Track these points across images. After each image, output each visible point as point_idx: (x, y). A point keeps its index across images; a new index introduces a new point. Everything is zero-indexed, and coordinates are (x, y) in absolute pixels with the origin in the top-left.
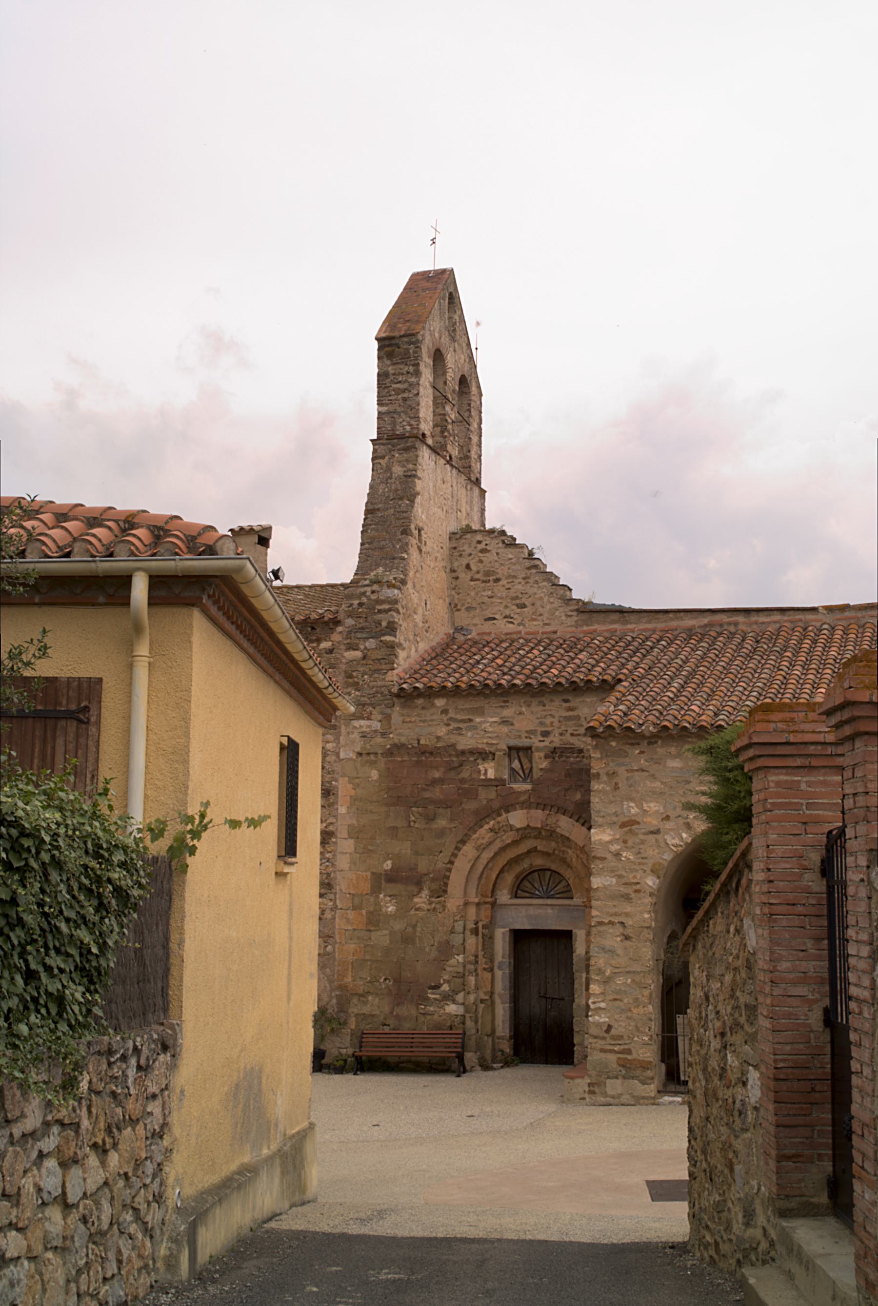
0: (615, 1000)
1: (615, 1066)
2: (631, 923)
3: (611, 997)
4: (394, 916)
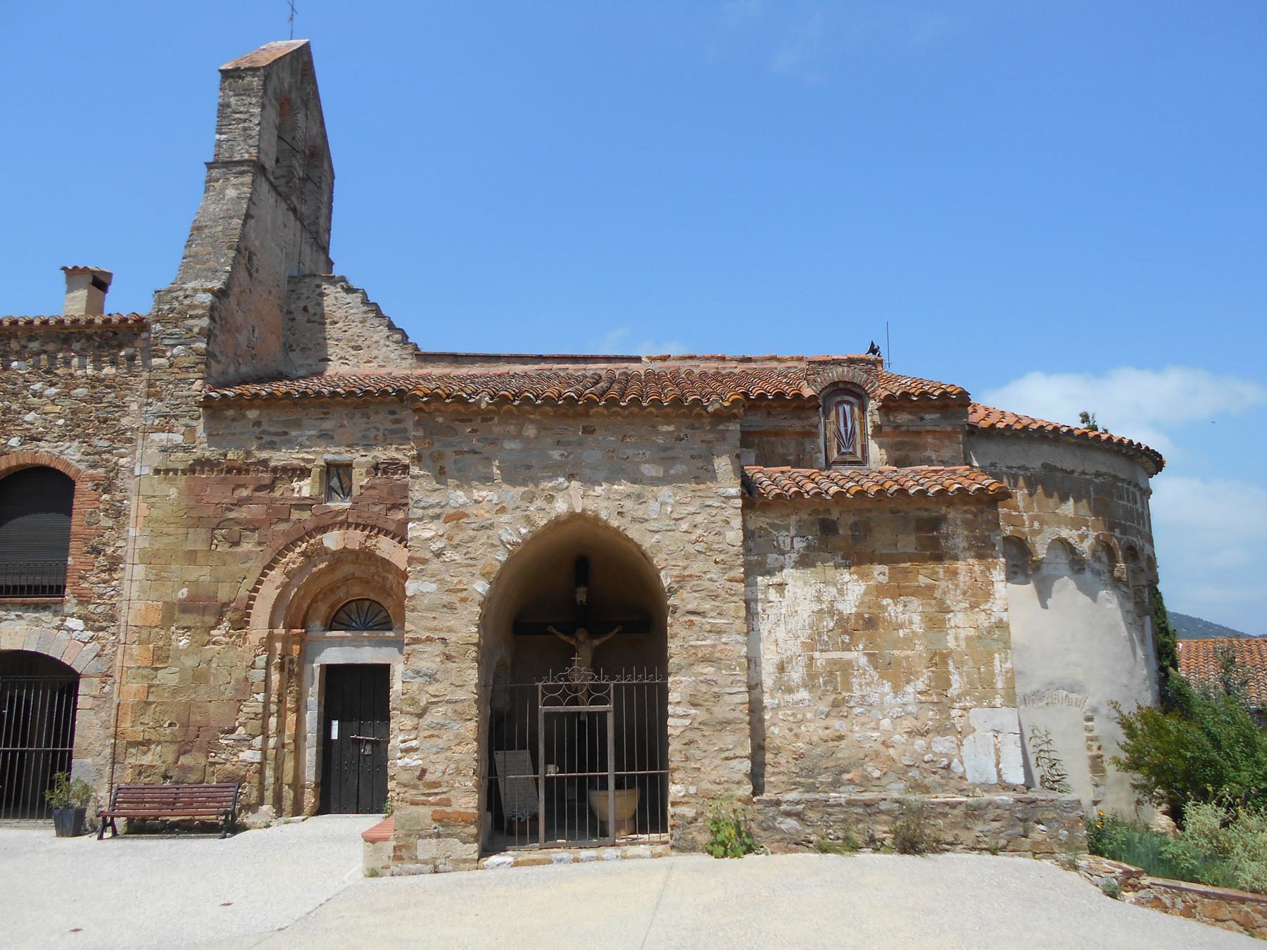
0: (432, 736)
1: (429, 821)
2: (454, 639)
3: (426, 733)
4: (186, 652)
